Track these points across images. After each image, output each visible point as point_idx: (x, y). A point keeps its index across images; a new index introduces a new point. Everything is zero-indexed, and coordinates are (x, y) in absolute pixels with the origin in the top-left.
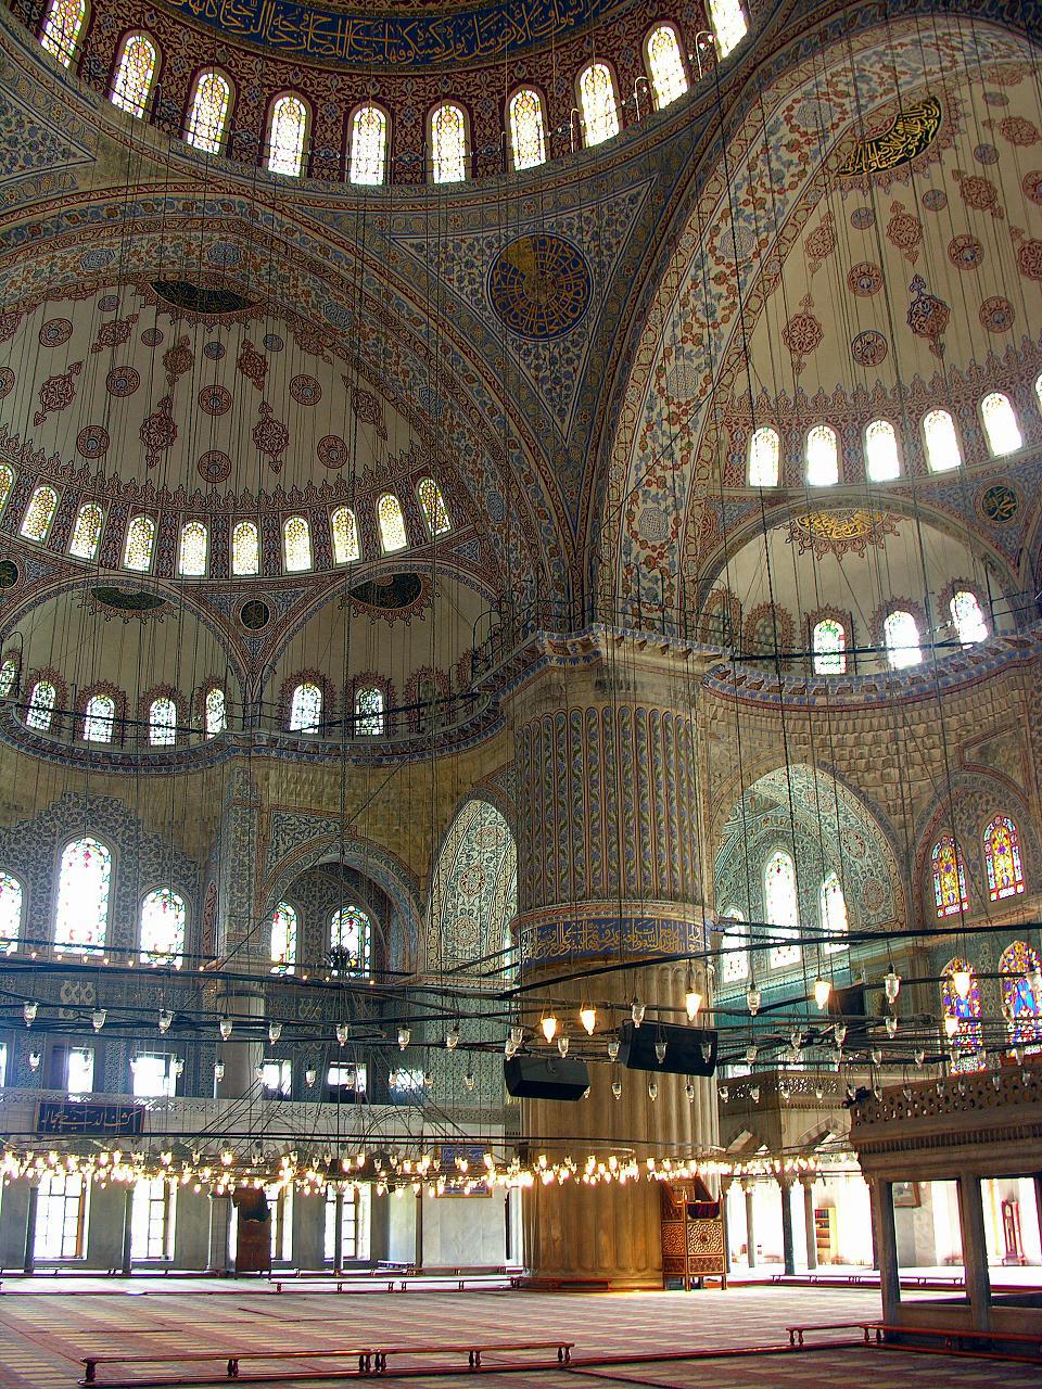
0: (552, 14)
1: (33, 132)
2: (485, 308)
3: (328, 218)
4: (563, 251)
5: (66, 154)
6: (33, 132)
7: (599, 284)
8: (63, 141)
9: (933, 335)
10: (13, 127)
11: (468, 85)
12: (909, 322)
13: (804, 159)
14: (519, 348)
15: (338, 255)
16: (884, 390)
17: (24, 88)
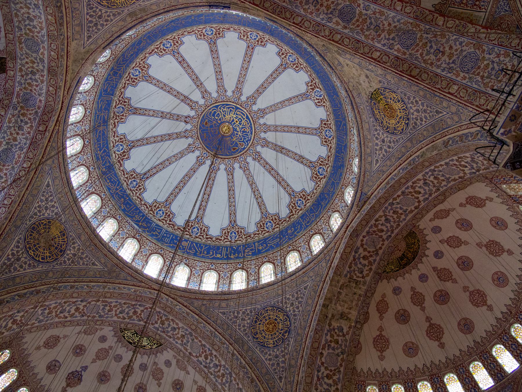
0: (122, 199)
1: (102, 25)
2: (30, 221)
3: (54, 145)
4: (64, 244)
5: (89, 37)
6: (102, 25)
7: (57, 264)
8: (95, 36)
9: (68, 385)
10: (106, 18)
11: (94, 177)
12: (69, 374)
13: (130, 318)
14: (18, 242)
15: (41, 153)
16: (40, 383)
17: (121, 23)
